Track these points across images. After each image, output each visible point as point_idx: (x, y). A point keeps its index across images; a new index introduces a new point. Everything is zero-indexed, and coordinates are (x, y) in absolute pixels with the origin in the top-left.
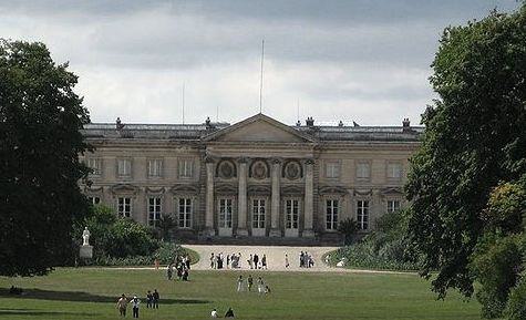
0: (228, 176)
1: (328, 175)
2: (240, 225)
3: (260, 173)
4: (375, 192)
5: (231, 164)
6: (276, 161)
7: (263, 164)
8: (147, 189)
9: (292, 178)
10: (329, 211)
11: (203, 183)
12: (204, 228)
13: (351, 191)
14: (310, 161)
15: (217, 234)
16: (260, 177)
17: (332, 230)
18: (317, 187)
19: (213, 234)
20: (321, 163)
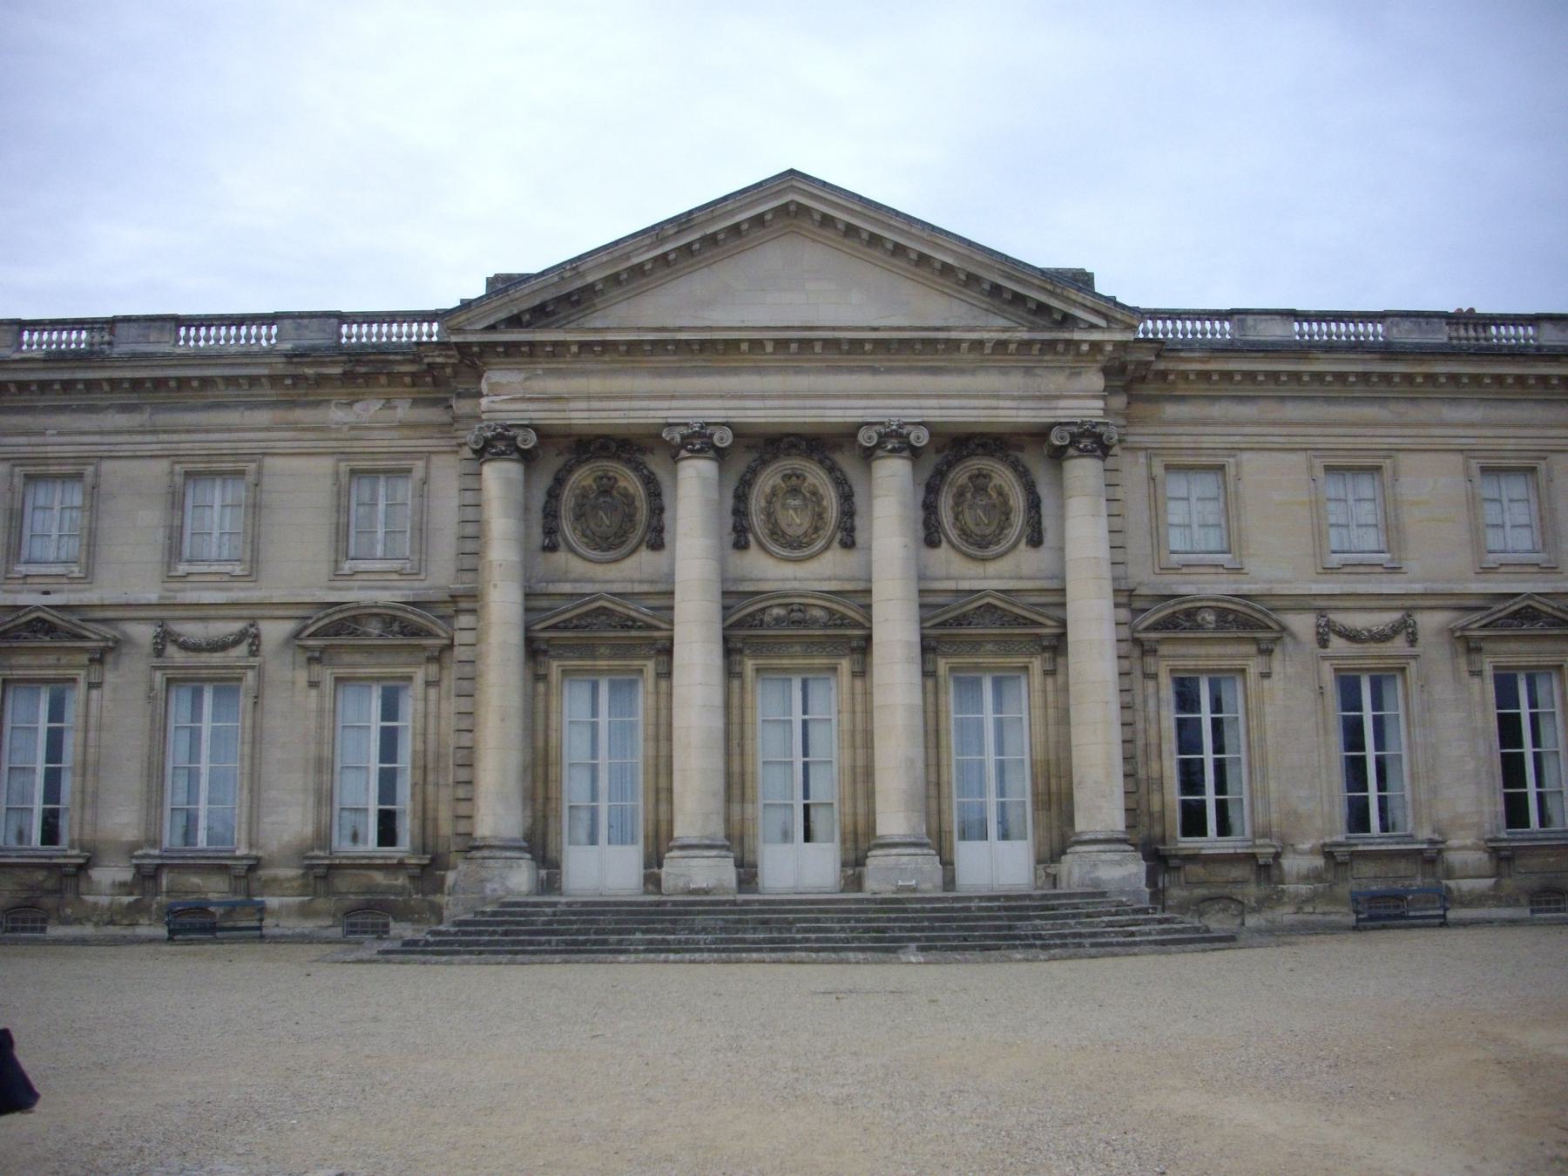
0: (611, 543)
1: (1176, 540)
2: (685, 829)
3: (795, 520)
4: (1429, 622)
5: (629, 481)
6: (895, 440)
7: (816, 476)
8: (165, 638)
9: (980, 544)
10: (1188, 737)
11: (466, 601)
12: (471, 847)
13: (1303, 624)
14: (1092, 441)
15: (550, 878)
16: (795, 546)
17: (1212, 842)
18: (1126, 597)
19: (519, 879)
20: (1133, 469)
